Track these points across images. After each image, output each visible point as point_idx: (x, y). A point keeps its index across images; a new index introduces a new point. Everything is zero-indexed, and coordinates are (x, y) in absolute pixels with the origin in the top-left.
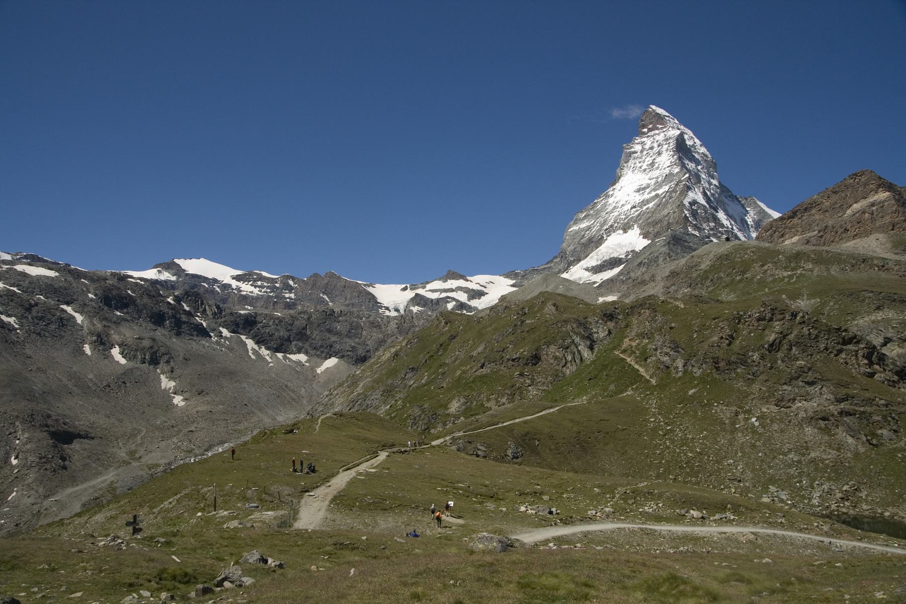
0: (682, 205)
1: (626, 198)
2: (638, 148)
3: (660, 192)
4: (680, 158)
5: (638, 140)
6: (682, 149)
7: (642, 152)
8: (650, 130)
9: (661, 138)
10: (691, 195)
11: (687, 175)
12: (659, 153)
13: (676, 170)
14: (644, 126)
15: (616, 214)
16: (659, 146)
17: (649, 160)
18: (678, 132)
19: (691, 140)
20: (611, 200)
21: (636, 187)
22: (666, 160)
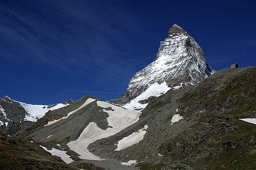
0: (187, 71)
1: (161, 67)
3: (177, 65)
5: (168, 40)
6: (188, 44)
7: (169, 45)
9: (179, 39)
10: (192, 67)
11: (191, 57)
12: (178, 47)
13: (185, 55)
15: (155, 74)
17: (172, 49)
18: (187, 37)
19: (193, 42)
20: (153, 68)
21: (166, 62)
22: (181, 50)
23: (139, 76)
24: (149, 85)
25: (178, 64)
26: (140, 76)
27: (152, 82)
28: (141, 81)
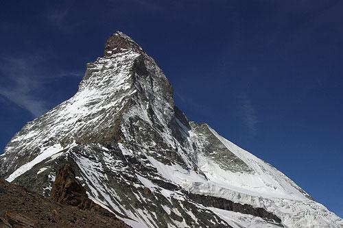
0: (119, 120)
1: (76, 112)
2: (100, 67)
3: (106, 107)
6: (138, 69)
7: (102, 70)
8: (114, 52)
10: (133, 112)
11: (135, 91)
12: (117, 72)
13: (127, 87)
14: (109, 49)
15: (61, 126)
17: (106, 78)
18: (137, 55)
19: (150, 65)
20: (61, 113)
21: (86, 101)
22: (121, 80)
23: (31, 130)
25: (109, 106)
26: (34, 128)
27: (50, 143)
28: (31, 139)
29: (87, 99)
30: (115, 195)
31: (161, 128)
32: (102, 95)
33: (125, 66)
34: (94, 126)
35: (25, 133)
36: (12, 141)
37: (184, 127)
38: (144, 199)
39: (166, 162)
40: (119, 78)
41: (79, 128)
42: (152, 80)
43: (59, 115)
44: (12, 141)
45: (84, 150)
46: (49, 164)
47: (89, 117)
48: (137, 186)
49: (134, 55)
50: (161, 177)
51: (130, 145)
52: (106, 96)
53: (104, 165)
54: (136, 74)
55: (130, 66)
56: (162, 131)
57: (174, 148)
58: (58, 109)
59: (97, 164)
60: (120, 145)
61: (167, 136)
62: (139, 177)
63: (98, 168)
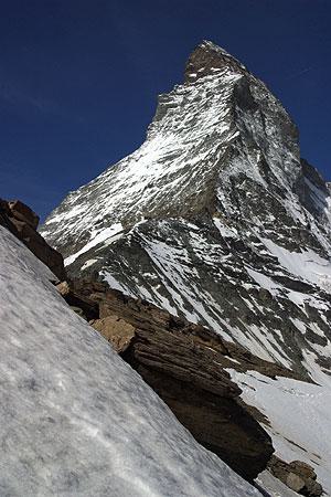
3: (192, 162)
4: (233, 112)
6: (240, 101)
7: (183, 104)
8: (201, 75)
10: (236, 167)
11: (238, 133)
12: (207, 106)
13: (224, 128)
14: (193, 70)
15: (121, 196)
16: (207, 96)
17: (190, 116)
18: (238, 77)
20: (121, 175)
21: (159, 154)
22: (214, 118)
23: (75, 204)
24: (93, 233)
25: (196, 159)
26: (79, 201)
28: (76, 218)
29: (161, 152)
30: (212, 302)
31: (282, 192)
32: (185, 143)
33: (219, 96)
34: (173, 194)
35: (66, 210)
36: (48, 223)
37: (318, 192)
38: (261, 308)
39: (292, 247)
40: (210, 116)
41: (149, 198)
42: (263, 116)
43: (118, 178)
44: (48, 223)
45: (158, 229)
46: (100, 253)
47: (165, 179)
48: (248, 286)
49: (233, 77)
50: (285, 272)
51: (232, 220)
52: (191, 145)
53: (191, 253)
54: (237, 108)
55: (227, 95)
56: (284, 198)
57: (305, 224)
58: (115, 169)
59: (180, 252)
60: (217, 221)
61: (292, 204)
62: (252, 273)
63: (182, 258)
